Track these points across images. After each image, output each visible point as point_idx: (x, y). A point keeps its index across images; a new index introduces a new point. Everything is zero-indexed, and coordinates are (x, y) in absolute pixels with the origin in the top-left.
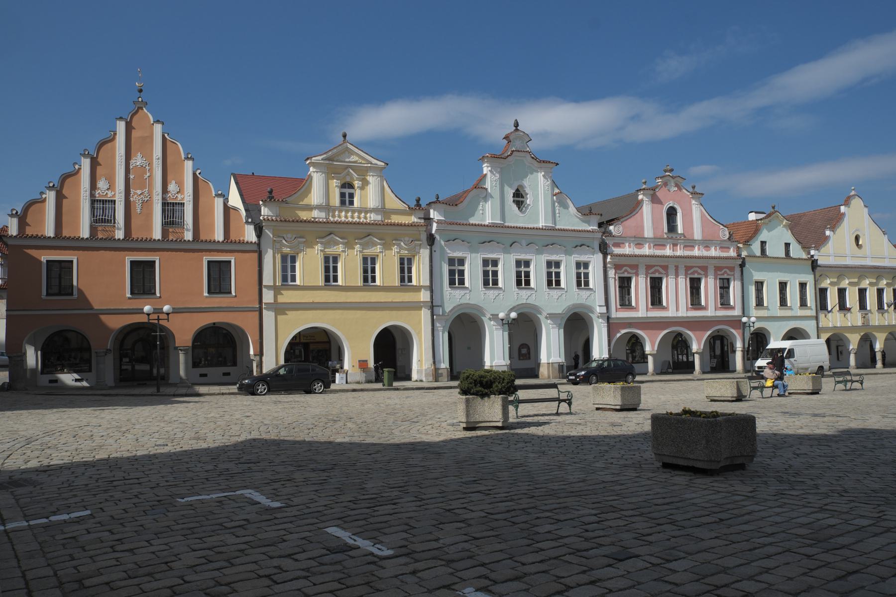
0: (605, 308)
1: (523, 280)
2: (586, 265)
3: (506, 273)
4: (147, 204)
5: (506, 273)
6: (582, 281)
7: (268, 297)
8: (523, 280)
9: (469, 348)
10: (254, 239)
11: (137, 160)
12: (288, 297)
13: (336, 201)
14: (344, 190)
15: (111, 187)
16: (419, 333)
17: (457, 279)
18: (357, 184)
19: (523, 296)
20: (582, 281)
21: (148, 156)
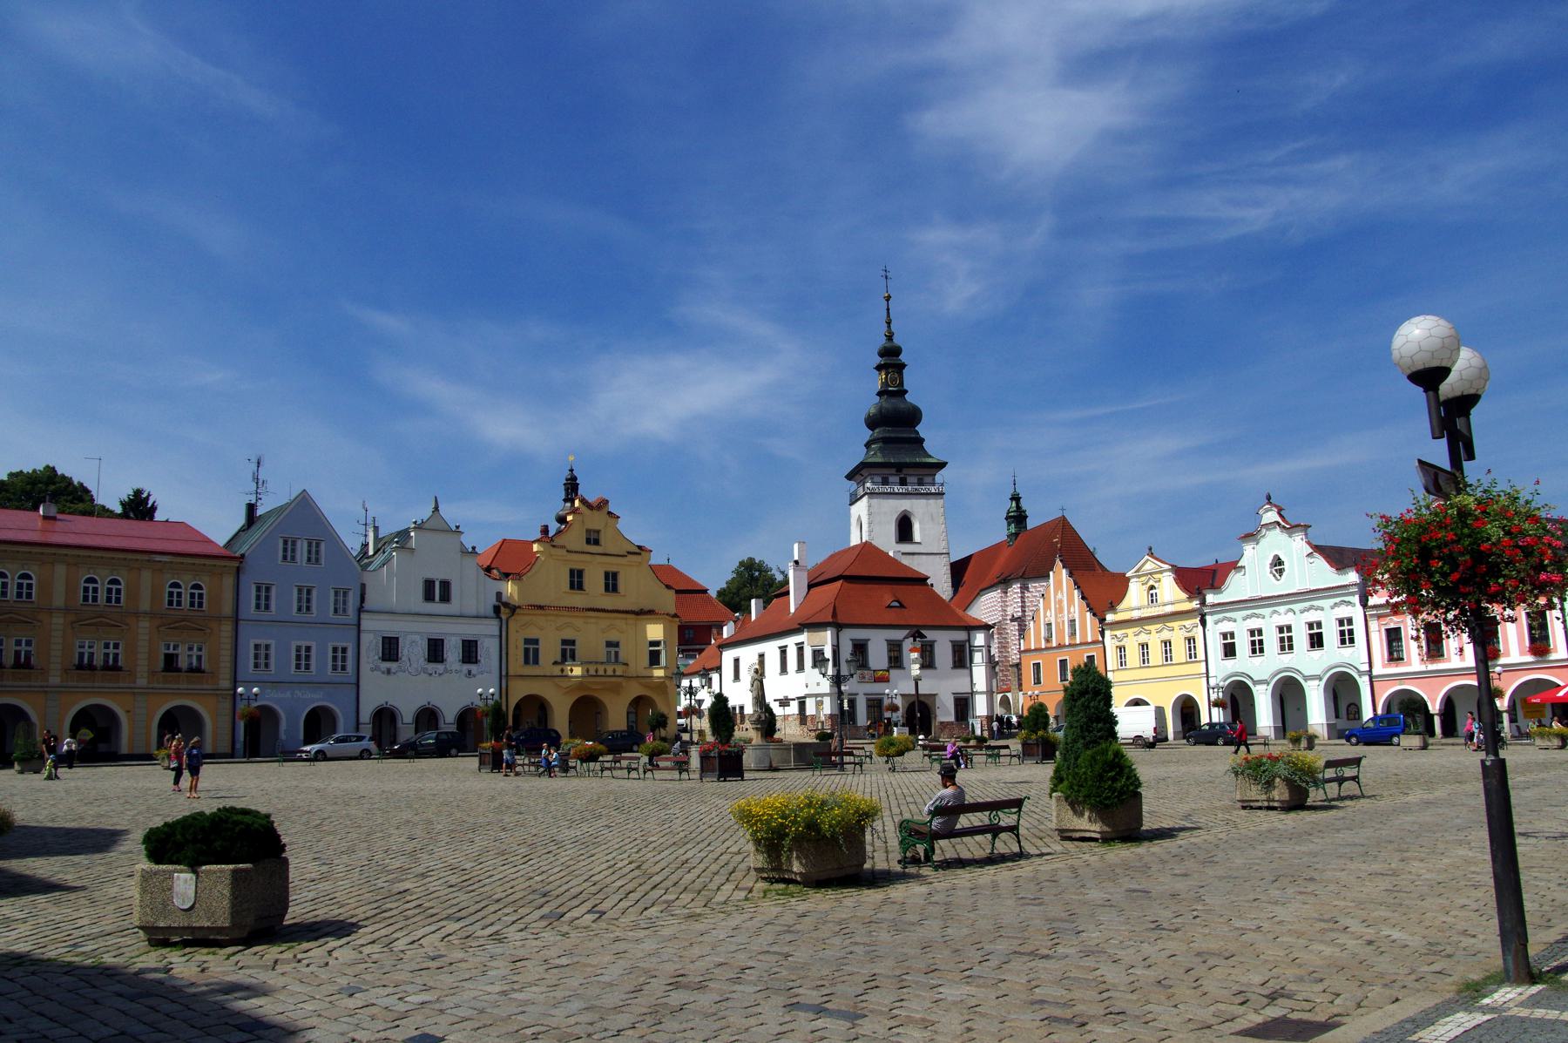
0: (1367, 665)
1: (1286, 645)
2: (1350, 621)
3: (1271, 640)
4: (1063, 621)
5: (1271, 640)
6: (1347, 638)
8: (1286, 645)
9: (1298, 709)
10: (1100, 639)
11: (1059, 596)
13: (1145, 600)
14: (1151, 592)
16: (1201, 699)
17: (1230, 651)
18: (1156, 585)
19: (1287, 660)
20: (1347, 638)
21: (1062, 592)
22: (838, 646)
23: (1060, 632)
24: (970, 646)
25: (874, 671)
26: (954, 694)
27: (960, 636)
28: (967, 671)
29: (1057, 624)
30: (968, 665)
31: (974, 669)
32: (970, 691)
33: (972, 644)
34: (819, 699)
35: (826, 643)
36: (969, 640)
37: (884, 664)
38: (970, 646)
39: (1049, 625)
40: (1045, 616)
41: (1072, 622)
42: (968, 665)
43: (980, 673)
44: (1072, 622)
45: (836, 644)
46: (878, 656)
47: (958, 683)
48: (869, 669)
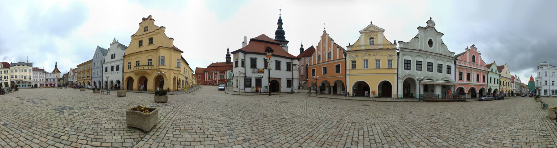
4: (325, 54)
7: (348, 72)
10: (344, 57)
11: (324, 45)
12: (354, 72)
15: (320, 53)
21: (326, 44)
22: (245, 60)
23: (324, 57)
24: (292, 64)
25: (259, 69)
26: (287, 79)
27: (289, 61)
28: (291, 72)
29: (323, 55)
30: (292, 70)
31: (293, 71)
32: (292, 78)
33: (293, 64)
34: (237, 78)
35: (239, 58)
36: (292, 63)
37: (263, 67)
38: (292, 64)
39: (319, 57)
40: (318, 53)
41: (329, 54)
42: (292, 70)
43: (296, 74)
44: (329, 54)
45: (244, 59)
46: (260, 64)
47: (288, 75)
48: (257, 68)
